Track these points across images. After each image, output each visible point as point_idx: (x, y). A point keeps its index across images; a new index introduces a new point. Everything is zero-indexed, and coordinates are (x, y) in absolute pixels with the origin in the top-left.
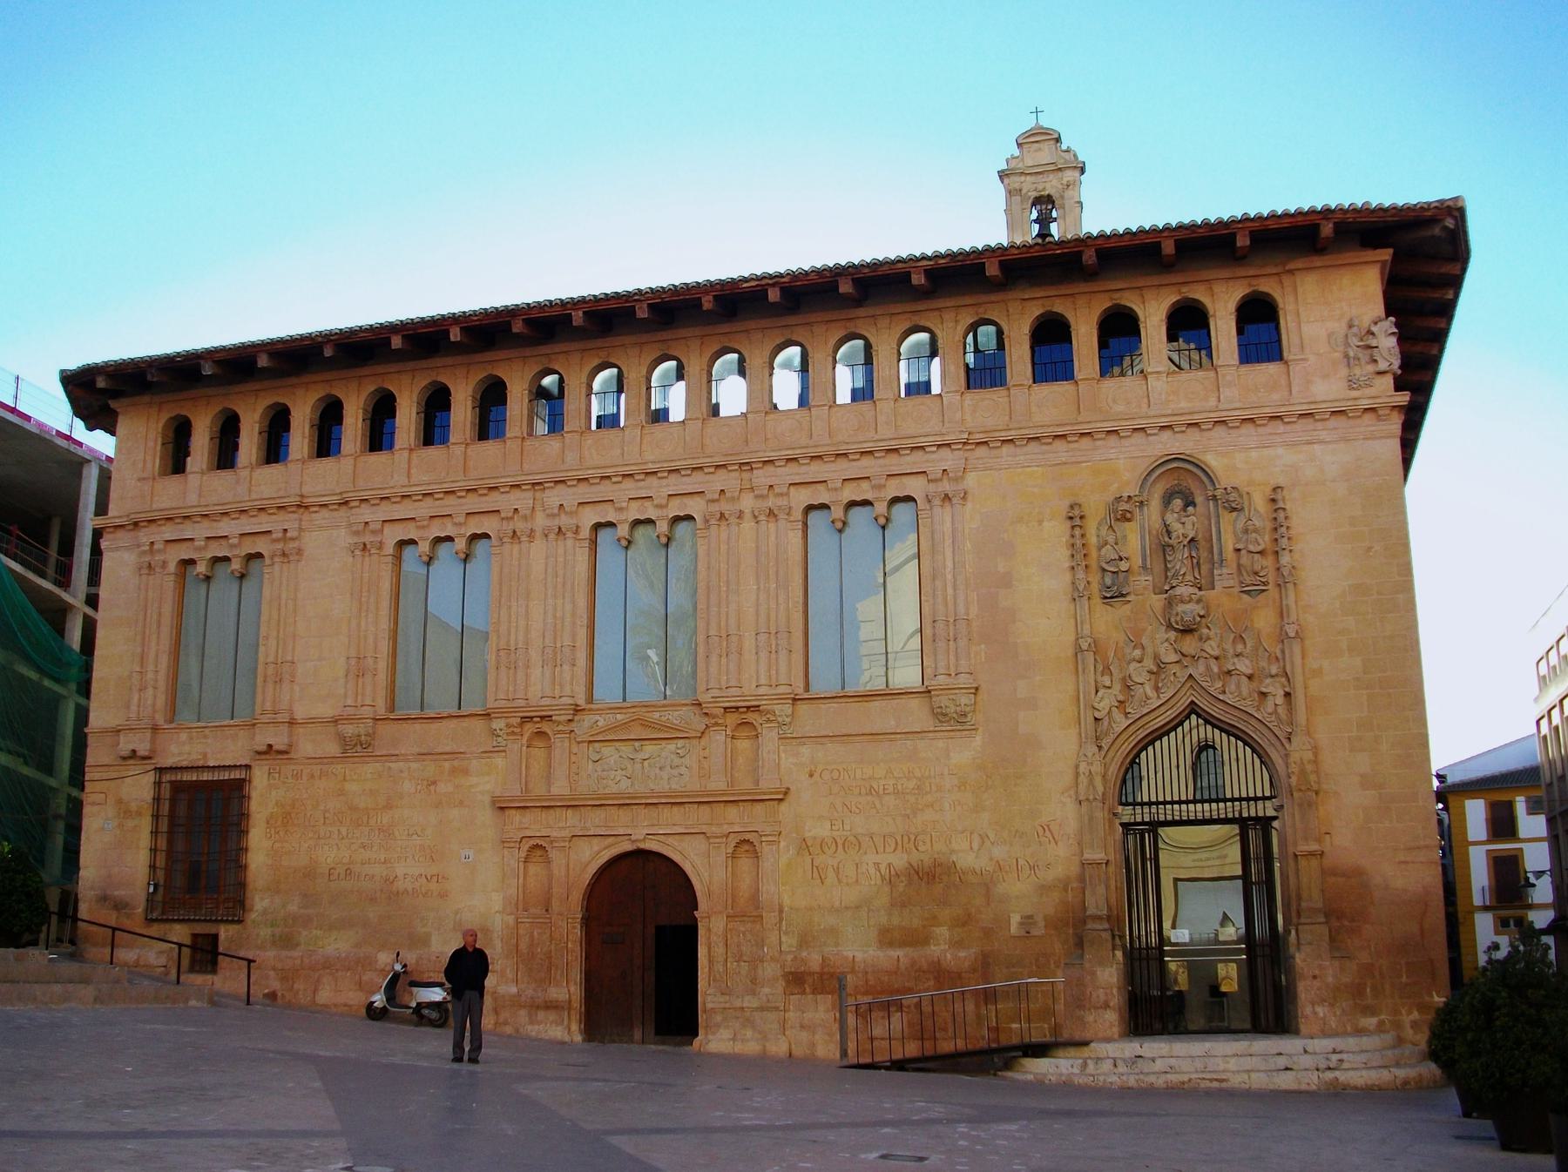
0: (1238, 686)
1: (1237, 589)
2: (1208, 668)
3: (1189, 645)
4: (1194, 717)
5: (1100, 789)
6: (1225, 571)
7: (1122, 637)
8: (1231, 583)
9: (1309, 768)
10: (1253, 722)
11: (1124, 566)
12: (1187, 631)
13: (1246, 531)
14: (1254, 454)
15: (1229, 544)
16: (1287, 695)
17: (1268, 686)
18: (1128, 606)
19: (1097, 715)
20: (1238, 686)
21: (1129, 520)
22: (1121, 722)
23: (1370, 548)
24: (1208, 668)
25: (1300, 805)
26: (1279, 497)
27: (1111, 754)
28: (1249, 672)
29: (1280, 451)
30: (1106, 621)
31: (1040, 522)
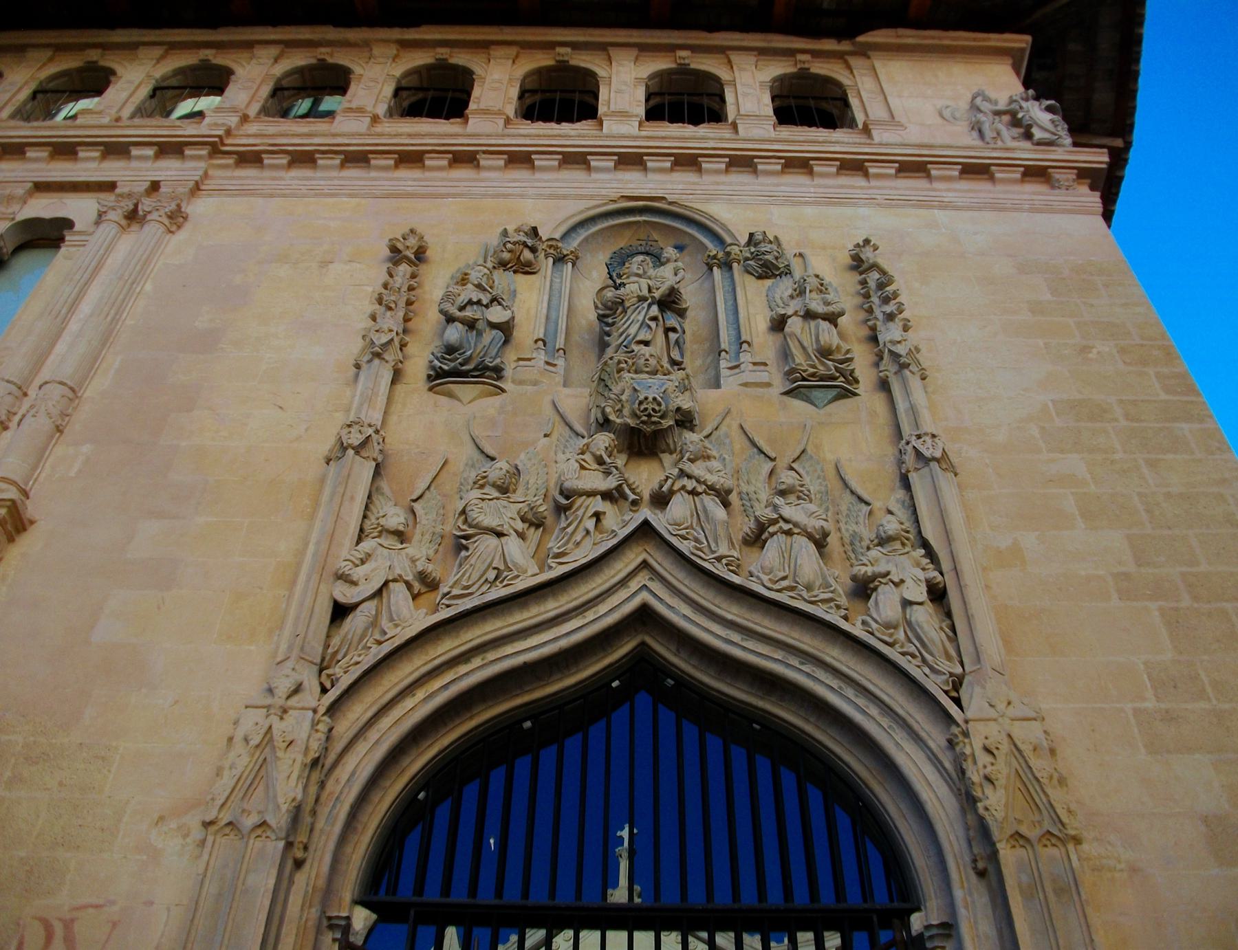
0: (787, 555)
1: (779, 385)
2: (700, 516)
3: (646, 476)
4: (643, 700)
5: (288, 784)
6: (745, 358)
7: (463, 454)
8: (763, 377)
9: (1040, 765)
10: (834, 654)
11: (497, 314)
12: (643, 440)
13: (801, 292)
14: (809, 211)
15: (757, 321)
16: (937, 594)
17: (876, 561)
18: (496, 401)
19: (346, 594)
20: (787, 555)
21: (526, 269)
22: (414, 618)
23: (1085, 349)
24: (700, 516)
25: (1029, 894)
26: (867, 254)
27: (358, 711)
28: (813, 524)
29: (863, 211)
30: (431, 427)
31: (325, 264)
